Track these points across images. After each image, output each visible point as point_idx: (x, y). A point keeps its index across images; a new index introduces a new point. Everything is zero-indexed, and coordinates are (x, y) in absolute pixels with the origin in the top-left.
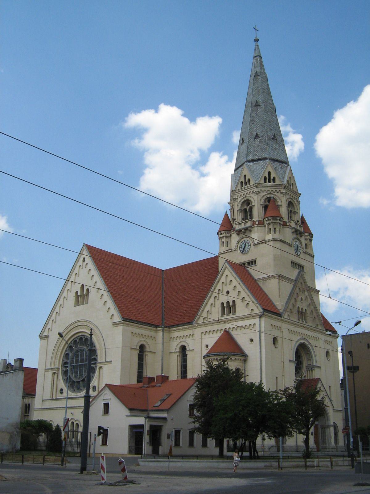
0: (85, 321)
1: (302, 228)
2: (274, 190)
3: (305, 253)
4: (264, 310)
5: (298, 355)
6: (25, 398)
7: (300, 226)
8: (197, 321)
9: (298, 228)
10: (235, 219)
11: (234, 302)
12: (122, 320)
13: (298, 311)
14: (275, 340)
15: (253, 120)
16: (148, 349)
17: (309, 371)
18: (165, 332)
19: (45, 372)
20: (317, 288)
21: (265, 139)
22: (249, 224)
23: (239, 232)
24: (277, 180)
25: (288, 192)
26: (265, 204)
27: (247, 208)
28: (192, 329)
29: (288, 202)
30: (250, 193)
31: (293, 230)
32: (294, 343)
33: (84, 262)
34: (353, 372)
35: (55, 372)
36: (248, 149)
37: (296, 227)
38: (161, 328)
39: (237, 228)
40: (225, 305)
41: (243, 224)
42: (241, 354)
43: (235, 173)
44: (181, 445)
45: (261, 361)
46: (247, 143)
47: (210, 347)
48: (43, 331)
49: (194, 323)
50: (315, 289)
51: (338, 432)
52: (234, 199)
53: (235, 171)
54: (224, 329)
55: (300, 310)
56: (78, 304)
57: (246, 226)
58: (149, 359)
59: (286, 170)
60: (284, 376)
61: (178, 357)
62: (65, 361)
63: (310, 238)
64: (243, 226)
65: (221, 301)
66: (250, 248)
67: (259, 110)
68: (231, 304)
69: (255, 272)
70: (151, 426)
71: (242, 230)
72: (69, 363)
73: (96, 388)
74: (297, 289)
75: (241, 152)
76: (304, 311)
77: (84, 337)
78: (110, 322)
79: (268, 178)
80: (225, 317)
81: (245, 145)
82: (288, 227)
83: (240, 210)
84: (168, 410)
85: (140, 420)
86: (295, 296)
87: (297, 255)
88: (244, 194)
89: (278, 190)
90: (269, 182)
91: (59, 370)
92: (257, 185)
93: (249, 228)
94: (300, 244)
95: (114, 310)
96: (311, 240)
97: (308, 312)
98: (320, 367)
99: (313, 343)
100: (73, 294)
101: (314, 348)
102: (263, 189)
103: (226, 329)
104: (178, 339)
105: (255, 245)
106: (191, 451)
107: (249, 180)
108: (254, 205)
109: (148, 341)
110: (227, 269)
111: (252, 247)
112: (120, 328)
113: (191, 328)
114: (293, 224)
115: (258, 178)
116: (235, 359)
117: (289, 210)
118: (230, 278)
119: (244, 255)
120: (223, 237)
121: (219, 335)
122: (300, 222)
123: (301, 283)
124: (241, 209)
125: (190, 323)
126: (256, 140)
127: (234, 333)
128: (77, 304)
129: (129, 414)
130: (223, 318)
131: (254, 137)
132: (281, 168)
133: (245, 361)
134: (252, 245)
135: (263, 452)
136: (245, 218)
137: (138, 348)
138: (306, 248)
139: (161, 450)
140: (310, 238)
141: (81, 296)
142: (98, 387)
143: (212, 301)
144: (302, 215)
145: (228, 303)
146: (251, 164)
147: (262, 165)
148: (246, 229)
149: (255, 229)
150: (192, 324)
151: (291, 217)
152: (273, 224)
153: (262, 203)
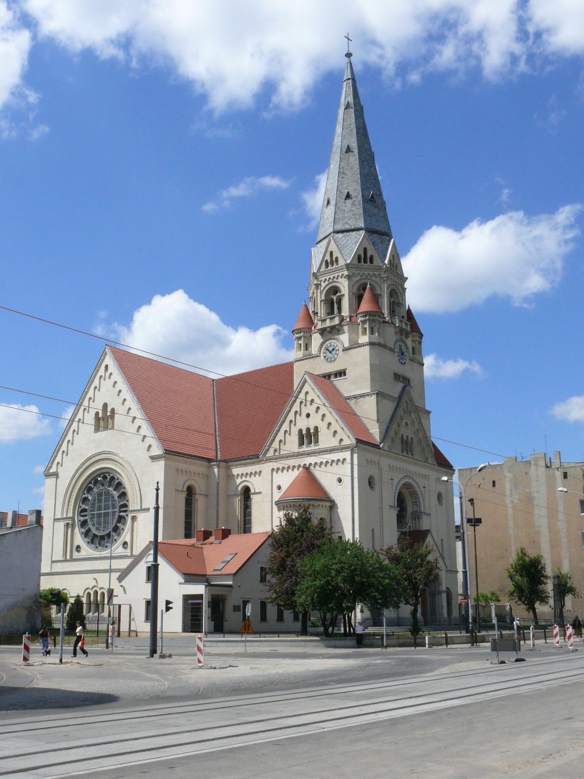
0: (110, 453)
1: (409, 326)
2: (371, 273)
3: (412, 360)
4: (359, 441)
5: (401, 501)
7: (406, 324)
9: (404, 327)
10: (317, 313)
11: (316, 428)
13: (402, 440)
15: (343, 173)
16: (198, 491)
17: (415, 519)
20: (427, 408)
23: (322, 332)
25: (390, 277)
30: (339, 278)
34: (474, 526)
35: (68, 522)
38: (216, 463)
39: (320, 326)
40: (304, 432)
41: (328, 321)
47: (284, 488)
49: (261, 456)
50: (425, 409)
52: (315, 284)
54: (302, 465)
55: (405, 438)
57: (332, 324)
58: (200, 503)
62: (82, 508)
63: (419, 339)
64: (328, 323)
65: (299, 426)
66: (337, 354)
68: (312, 431)
69: (344, 386)
71: (328, 329)
72: (88, 511)
73: (127, 545)
75: (326, 217)
76: (410, 440)
77: (109, 475)
78: (147, 455)
80: (305, 448)
82: (390, 326)
85: (199, 589)
87: (402, 363)
90: (365, 262)
92: (348, 267)
96: (420, 343)
97: (415, 441)
98: (429, 515)
99: (421, 482)
101: (423, 489)
102: (356, 272)
105: (345, 350)
107: (337, 258)
108: (343, 295)
111: (341, 353)
112: (162, 463)
115: (350, 257)
116: (319, 505)
121: (296, 473)
122: (406, 318)
123: (406, 401)
127: (318, 473)
128: (97, 429)
129: (183, 581)
130: (302, 450)
131: (344, 197)
132: (382, 242)
134: (341, 350)
136: (331, 312)
137: (185, 489)
138: (414, 353)
143: (286, 426)
144: (409, 307)
145: (308, 429)
146: (340, 235)
147: (356, 238)
148: (333, 328)
151: (393, 311)
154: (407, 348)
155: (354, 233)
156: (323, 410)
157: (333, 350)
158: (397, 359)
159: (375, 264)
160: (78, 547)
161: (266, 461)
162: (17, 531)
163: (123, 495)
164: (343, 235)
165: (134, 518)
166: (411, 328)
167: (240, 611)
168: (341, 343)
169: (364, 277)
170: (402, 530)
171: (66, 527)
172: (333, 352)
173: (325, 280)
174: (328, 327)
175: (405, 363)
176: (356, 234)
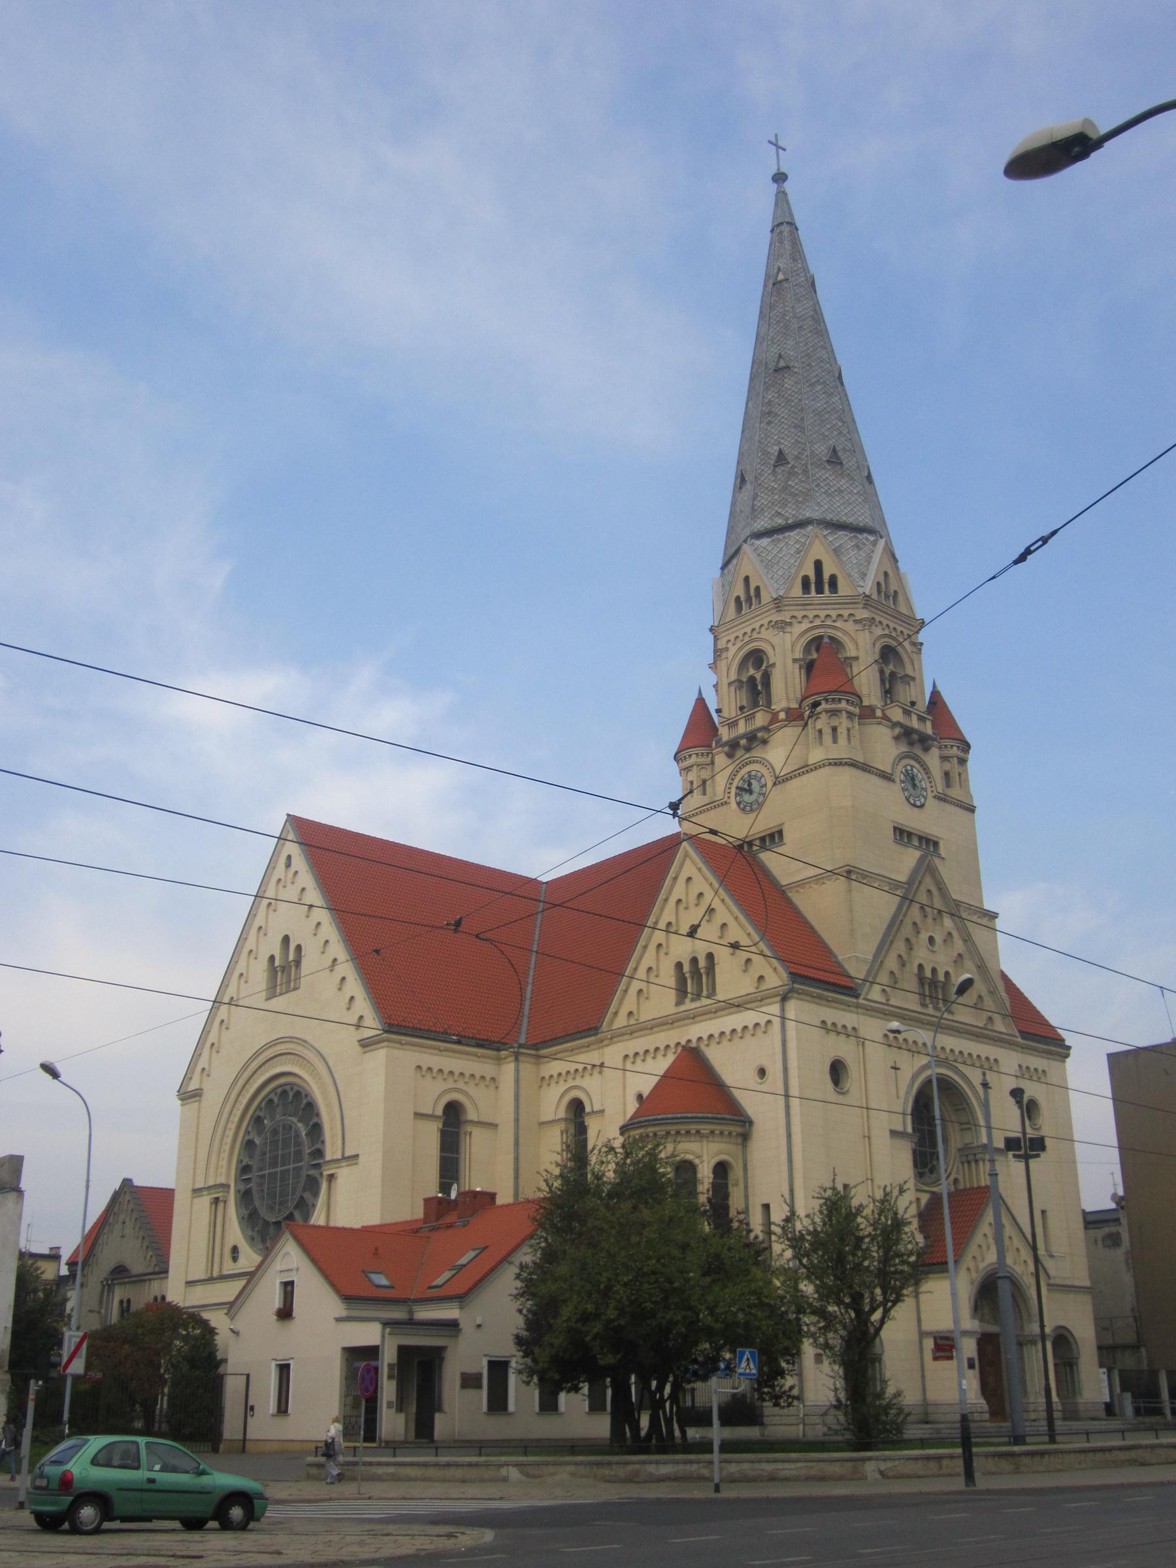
0: (292, 1039)
1: (929, 724)
2: (834, 614)
3: (942, 798)
6: (154, 1279)
7: (921, 719)
8: (612, 1022)
9: (915, 723)
11: (710, 957)
13: (921, 978)
14: (837, 1070)
15: (770, 413)
16: (472, 1115)
17: (969, 1162)
18: (523, 1062)
19: (193, 1198)
21: (806, 465)
22: (761, 719)
25: (878, 619)
26: (810, 657)
28: (599, 1048)
29: (878, 646)
30: (763, 629)
31: (897, 730)
34: (1026, 1158)
35: (216, 1196)
36: (754, 499)
37: (908, 723)
39: (725, 738)
40: (686, 968)
41: (742, 723)
42: (728, 1117)
43: (722, 575)
44: (511, 1407)
45: (789, 1136)
46: (752, 483)
48: (187, 1078)
51: (1078, 1358)
53: (723, 568)
55: (928, 974)
56: (276, 993)
59: (873, 551)
60: (872, 1180)
62: (244, 1163)
64: (742, 728)
67: (788, 383)
68: (702, 963)
70: (403, 1351)
72: (255, 1168)
74: (915, 910)
76: (941, 977)
80: (688, 1005)
81: (748, 486)
82: (879, 723)
83: (733, 682)
84: (461, 1298)
85: (368, 1334)
86: (907, 930)
87: (914, 805)
88: (745, 633)
91: (228, 1192)
93: (759, 735)
94: (921, 770)
95: (364, 1007)
100: (263, 963)
102: (799, 614)
106: (496, 1428)
107: (758, 589)
108: (774, 665)
109: (471, 1089)
110: (688, 859)
112: (380, 1054)
114: (896, 714)
117: (887, 672)
118: (700, 885)
124: (739, 681)
125: (593, 1030)
126: (779, 470)
127: (716, 1056)
128: (272, 991)
131: (772, 462)
132: (857, 546)
133: (745, 1137)
135: (804, 1425)
137: (439, 1111)
139: (441, 1425)
140: (962, 754)
141: (283, 969)
143: (648, 959)
144: (934, 685)
145: (694, 961)
146: (765, 542)
148: (752, 737)
152: (829, 714)
153: (798, 654)
154: (927, 770)
155: (793, 534)
158: (901, 797)
159: (840, 593)
160: (235, 1250)
161: (611, 1039)
163: (316, 1130)
164: (769, 540)
165: (331, 1177)
166: (933, 727)
167: (480, 1386)
168: (771, 770)
169: (817, 622)
170: (934, 1189)
171: (213, 1206)
173: (737, 637)
174: (743, 736)
175: (922, 806)
176: (798, 534)
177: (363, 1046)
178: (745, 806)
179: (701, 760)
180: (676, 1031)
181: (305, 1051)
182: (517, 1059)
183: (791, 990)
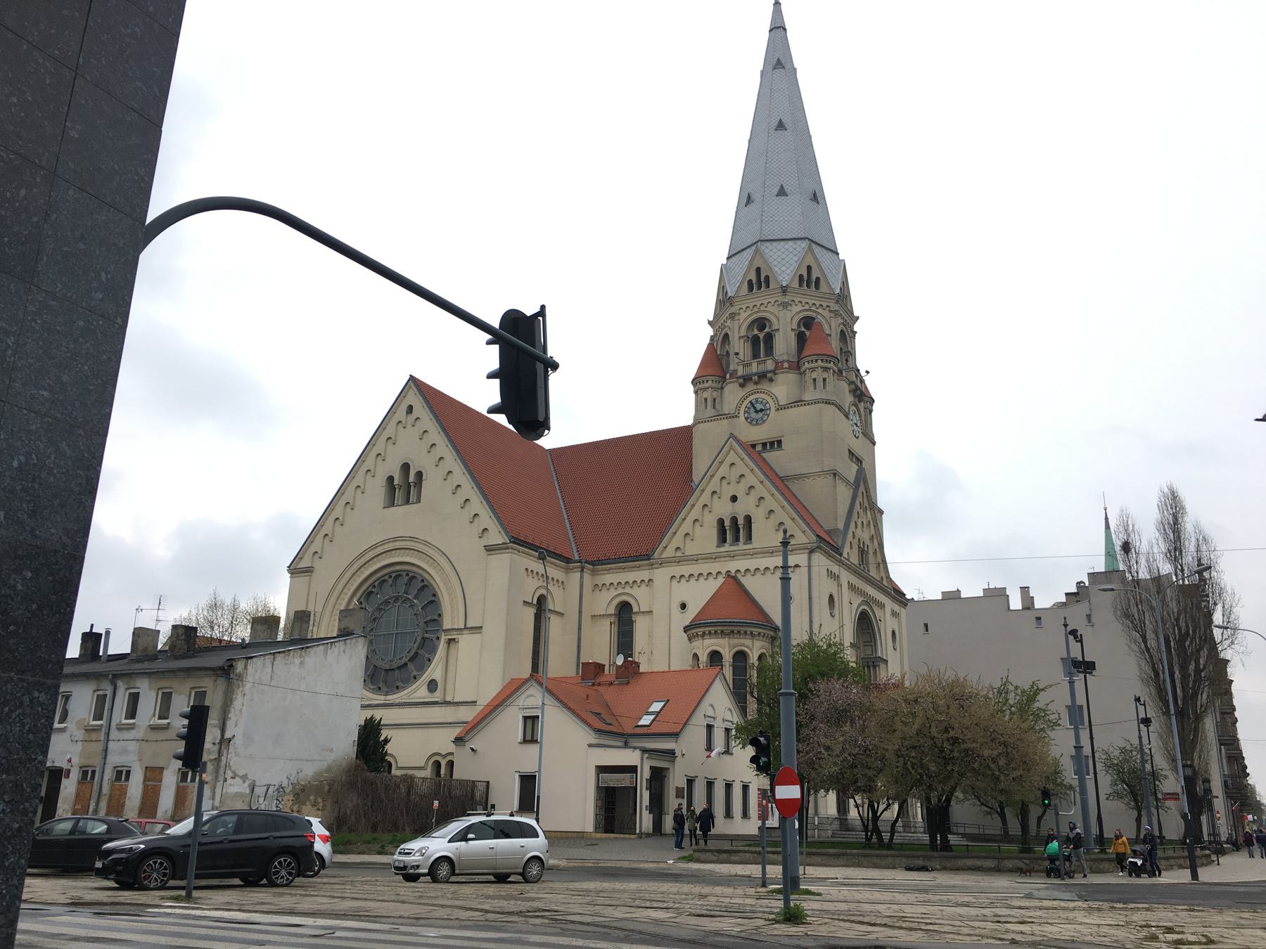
0: (412, 539)
2: (818, 303)
8: (661, 554)
11: (748, 519)
12: (511, 542)
17: (869, 667)
22: (770, 365)
24: (822, 283)
27: (759, 335)
28: (649, 569)
30: (769, 305)
32: (855, 606)
33: (409, 415)
39: (740, 373)
40: (727, 523)
41: (755, 365)
54: (724, 572)
57: (762, 368)
61: (613, 625)
64: (754, 368)
68: (741, 521)
79: (805, 277)
80: (727, 547)
83: (744, 336)
89: (825, 304)
93: (769, 375)
103: (729, 571)
104: (612, 589)
111: (773, 413)
113: (647, 567)
116: (759, 634)
118: (741, 468)
119: (755, 427)
120: (705, 389)
121: (713, 586)
125: (648, 557)
127: (749, 582)
128: (391, 502)
136: (756, 355)
137: (535, 602)
142: (443, 682)
143: (695, 513)
145: (734, 520)
148: (762, 376)
149: (781, 377)
150: (649, 559)
153: (795, 327)
156: (761, 490)
157: (762, 410)
161: (661, 564)
162: (328, 643)
167: (683, 797)
169: (807, 307)
172: (761, 415)
174: (755, 375)
177: (487, 550)
178: (752, 421)
179: (715, 385)
180: (717, 564)
181: (430, 550)
182: (582, 571)
183: (819, 547)
